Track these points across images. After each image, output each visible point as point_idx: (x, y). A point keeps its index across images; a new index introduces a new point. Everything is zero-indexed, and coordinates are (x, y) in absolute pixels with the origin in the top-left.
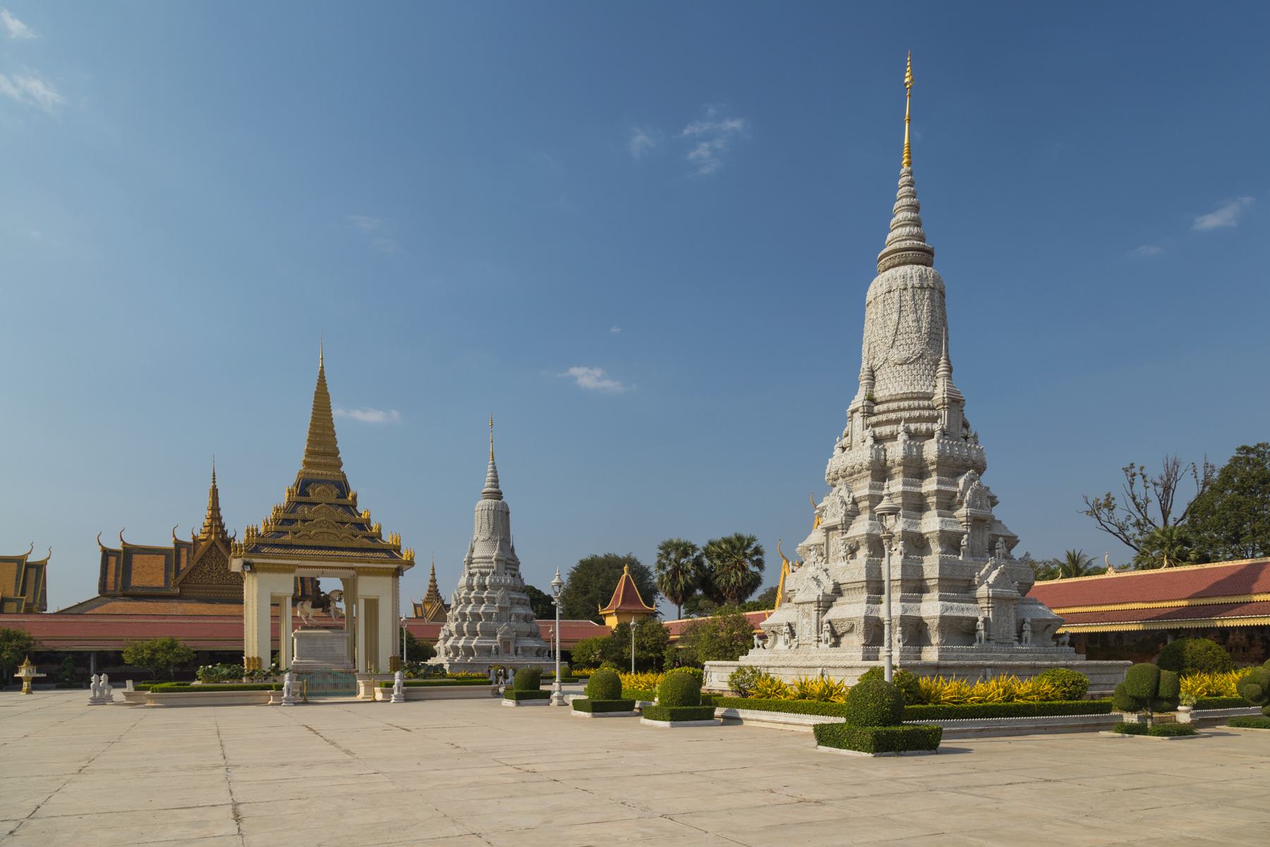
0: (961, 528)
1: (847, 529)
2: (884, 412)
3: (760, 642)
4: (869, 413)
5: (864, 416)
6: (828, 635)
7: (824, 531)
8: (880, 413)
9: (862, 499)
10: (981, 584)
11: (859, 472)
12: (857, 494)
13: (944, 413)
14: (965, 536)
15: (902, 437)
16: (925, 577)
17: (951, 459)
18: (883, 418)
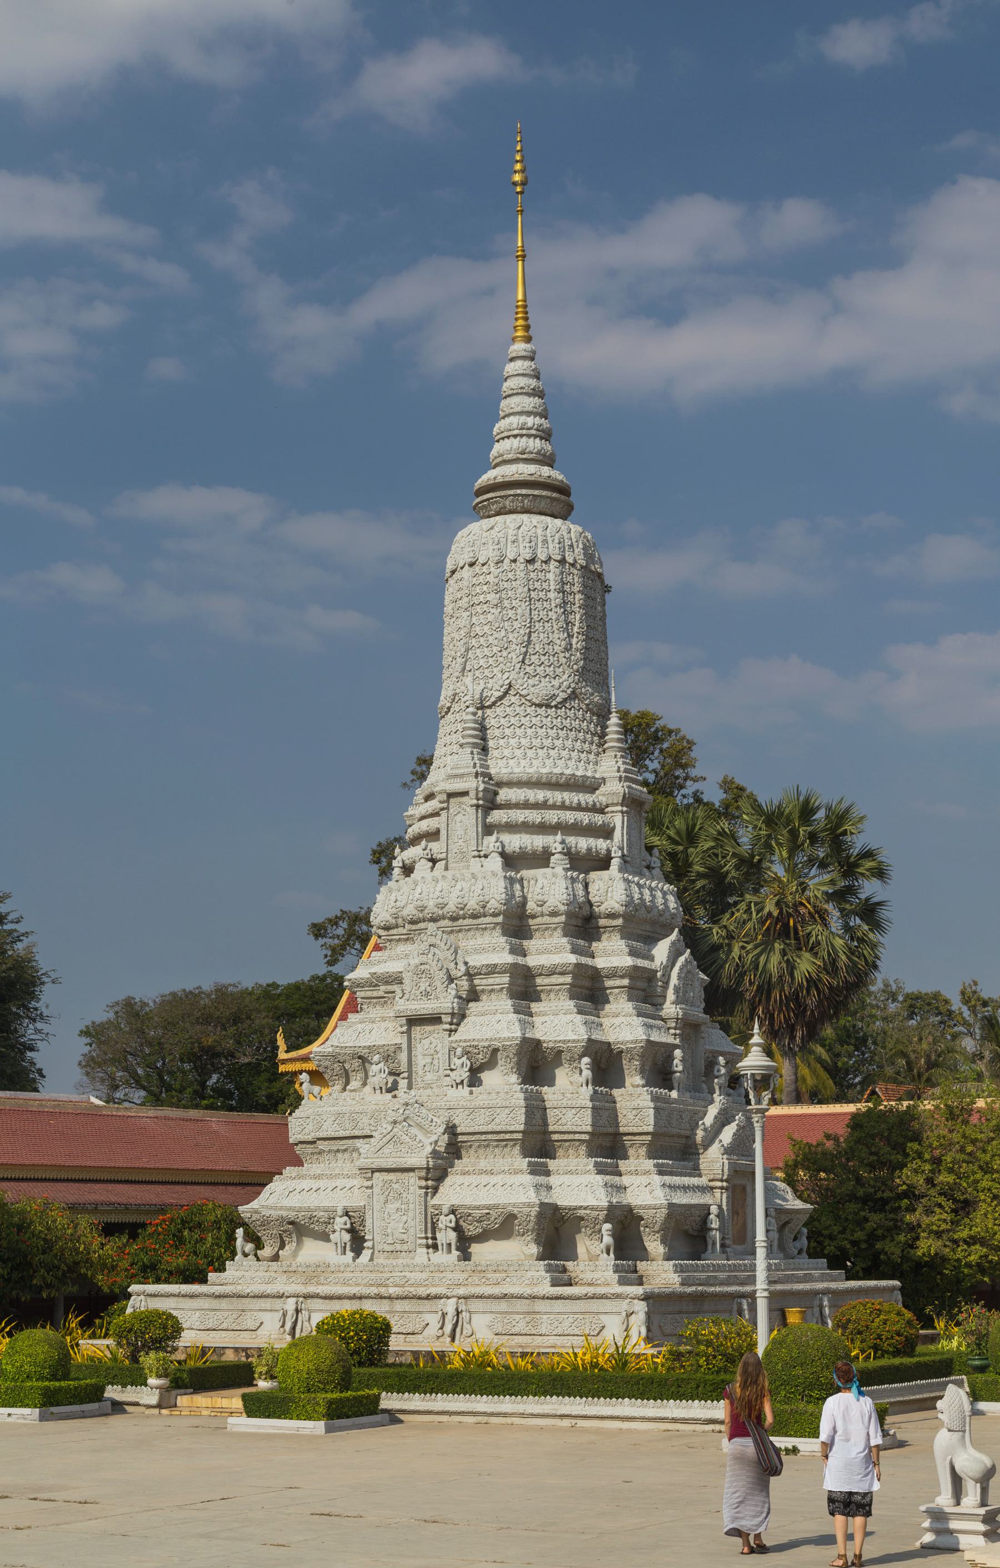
0: (670, 1040)
1: (458, 1024)
2: (517, 806)
3: (249, 1247)
4: (489, 803)
5: (478, 806)
6: (452, 1236)
7: (404, 1021)
8: (508, 806)
9: (492, 970)
10: (707, 1144)
11: (474, 916)
12: (477, 961)
13: (618, 821)
14: (678, 1053)
15: (559, 863)
16: (622, 1130)
17: (643, 911)
18: (520, 816)
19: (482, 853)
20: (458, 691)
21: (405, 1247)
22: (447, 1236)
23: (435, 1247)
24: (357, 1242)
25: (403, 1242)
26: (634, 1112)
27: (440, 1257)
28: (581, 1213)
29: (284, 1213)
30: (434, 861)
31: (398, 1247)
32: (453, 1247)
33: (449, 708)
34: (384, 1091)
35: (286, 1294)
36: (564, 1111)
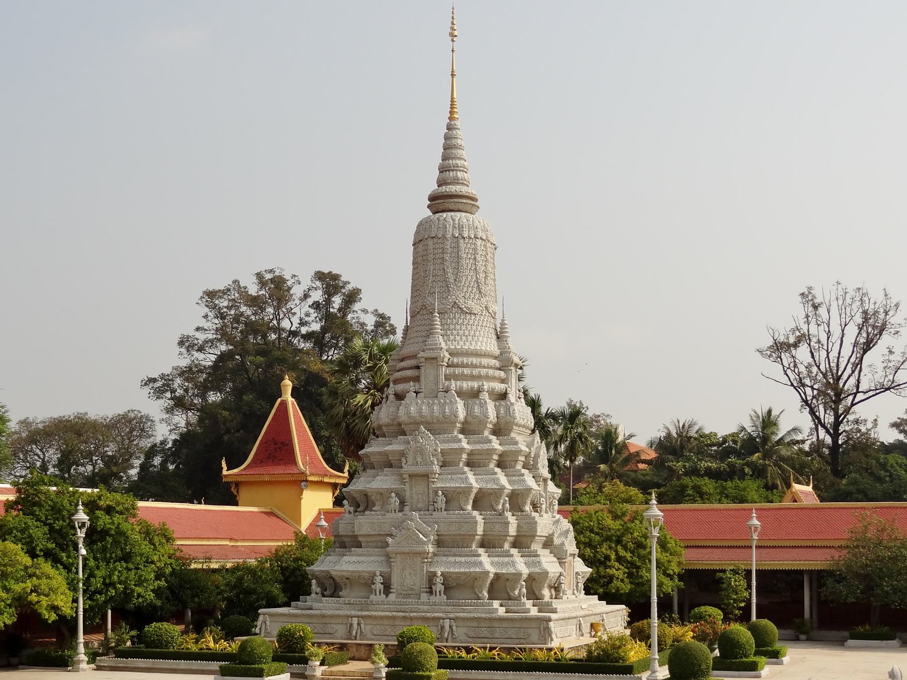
19: (444, 390)
20: (425, 304)
21: (414, 593)
22: (439, 587)
23: (431, 592)
24: (387, 588)
25: (412, 589)
26: (527, 525)
27: (433, 599)
28: (508, 577)
29: (344, 574)
30: (417, 393)
31: (410, 592)
32: (442, 593)
33: (419, 312)
34: (397, 511)
35: (351, 616)
36: (495, 524)
